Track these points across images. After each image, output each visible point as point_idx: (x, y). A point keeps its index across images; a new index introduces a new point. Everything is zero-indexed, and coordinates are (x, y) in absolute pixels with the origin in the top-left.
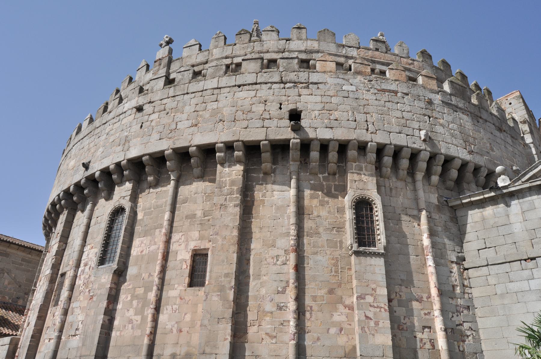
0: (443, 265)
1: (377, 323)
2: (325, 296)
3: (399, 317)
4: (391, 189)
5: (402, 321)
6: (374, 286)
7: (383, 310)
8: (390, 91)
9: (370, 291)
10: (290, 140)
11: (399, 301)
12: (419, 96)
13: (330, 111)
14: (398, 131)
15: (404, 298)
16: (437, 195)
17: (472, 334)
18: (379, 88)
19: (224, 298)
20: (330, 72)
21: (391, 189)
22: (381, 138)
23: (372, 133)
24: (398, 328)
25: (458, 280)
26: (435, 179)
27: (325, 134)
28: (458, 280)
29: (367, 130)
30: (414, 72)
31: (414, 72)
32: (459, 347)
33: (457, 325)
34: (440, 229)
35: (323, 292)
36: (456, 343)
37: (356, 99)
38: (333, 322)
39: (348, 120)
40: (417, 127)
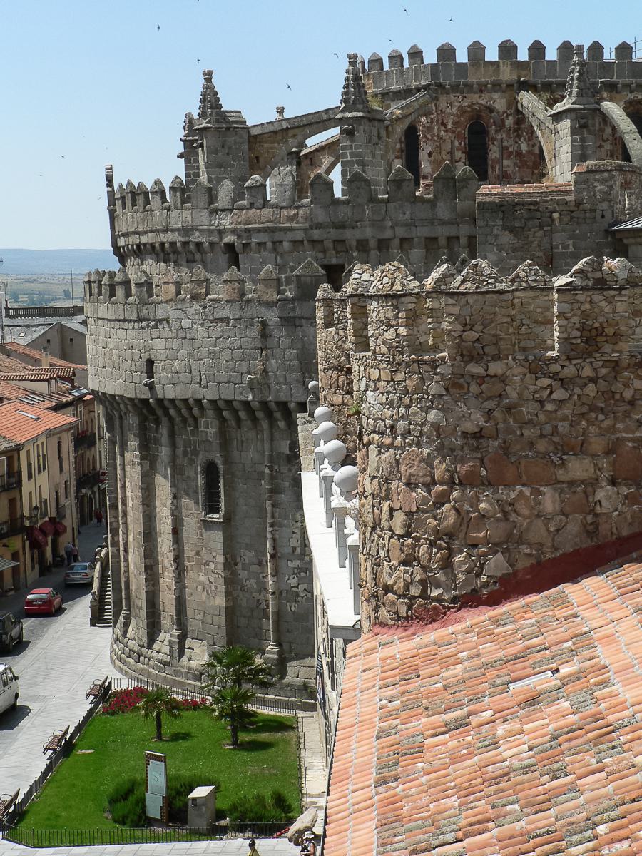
0: (284, 526)
1: (216, 587)
2: (195, 557)
3: (242, 579)
4: (242, 442)
5: (244, 583)
6: (214, 554)
7: (220, 576)
8: (221, 320)
9: (212, 559)
10: (149, 400)
11: (243, 564)
12: (253, 319)
13: (172, 360)
14: (226, 380)
15: (247, 561)
16: (289, 442)
17: (306, 595)
18: (211, 318)
19: (140, 555)
20: (172, 300)
21: (242, 442)
22: (209, 394)
23: (204, 387)
24: (241, 590)
25: (299, 542)
26: (282, 424)
27: (169, 393)
28: (299, 542)
29: (200, 383)
30: (298, 230)
31: (298, 230)
32: (290, 608)
33: (292, 587)
34: (287, 484)
35: (192, 554)
36: (288, 604)
37: (192, 339)
38: (199, 581)
39: (185, 372)
40: (245, 370)
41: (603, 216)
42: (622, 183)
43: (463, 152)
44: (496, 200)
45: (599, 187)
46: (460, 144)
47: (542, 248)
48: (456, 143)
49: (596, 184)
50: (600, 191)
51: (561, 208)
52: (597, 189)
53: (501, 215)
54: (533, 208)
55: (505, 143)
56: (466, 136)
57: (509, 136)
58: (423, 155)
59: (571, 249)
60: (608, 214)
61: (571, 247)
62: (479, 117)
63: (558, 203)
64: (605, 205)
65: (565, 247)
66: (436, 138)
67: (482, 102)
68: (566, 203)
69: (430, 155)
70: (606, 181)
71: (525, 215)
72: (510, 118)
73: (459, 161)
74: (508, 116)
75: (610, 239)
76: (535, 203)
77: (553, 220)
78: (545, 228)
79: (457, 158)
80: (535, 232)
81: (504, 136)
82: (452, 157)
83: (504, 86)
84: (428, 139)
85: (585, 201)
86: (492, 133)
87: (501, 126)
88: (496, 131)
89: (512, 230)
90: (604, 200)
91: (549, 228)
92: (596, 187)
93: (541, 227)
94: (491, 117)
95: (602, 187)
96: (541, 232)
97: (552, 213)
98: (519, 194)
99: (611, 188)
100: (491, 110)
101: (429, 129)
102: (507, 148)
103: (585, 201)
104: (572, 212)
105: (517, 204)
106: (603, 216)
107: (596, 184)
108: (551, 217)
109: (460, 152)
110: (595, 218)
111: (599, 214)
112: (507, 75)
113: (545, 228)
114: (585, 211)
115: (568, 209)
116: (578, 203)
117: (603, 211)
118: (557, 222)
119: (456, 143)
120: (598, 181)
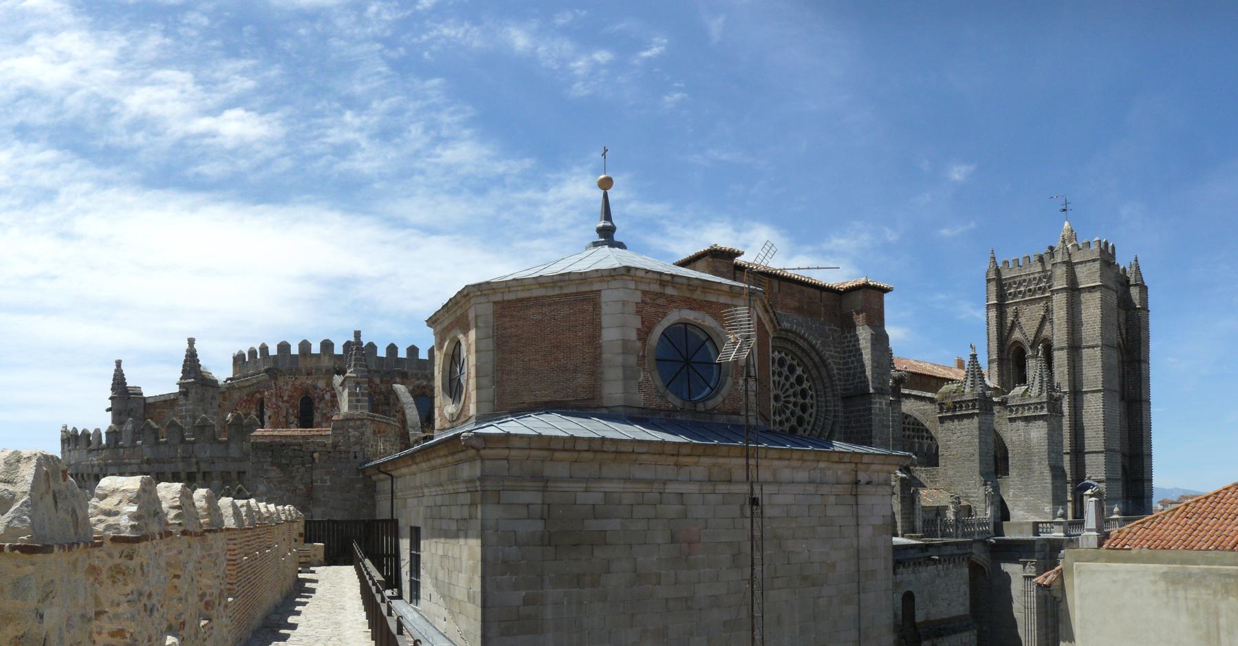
41: (356, 457)
42: (374, 431)
43: (295, 417)
44: (267, 441)
45: (352, 432)
46: (293, 411)
47: (304, 481)
48: (291, 411)
49: (350, 430)
50: (353, 436)
51: (321, 449)
52: (351, 434)
53: (270, 453)
54: (296, 448)
55: (325, 411)
56: (299, 405)
57: (327, 405)
58: (266, 418)
59: (328, 483)
60: (360, 455)
61: (328, 481)
62: (307, 392)
63: (318, 444)
64: (357, 448)
65: (323, 481)
66: (274, 406)
67: (308, 382)
68: (325, 445)
69: (270, 417)
70: (359, 428)
71: (291, 454)
72: (328, 393)
73: (292, 423)
74: (327, 391)
75: (361, 476)
76: (300, 445)
77: (313, 459)
78: (307, 466)
79: (291, 421)
80: (298, 469)
81: (324, 406)
82: (287, 420)
83: (324, 370)
84: (269, 407)
85: (340, 444)
86: (316, 405)
87: (322, 399)
88: (319, 402)
89: (280, 466)
90: (356, 443)
91: (310, 465)
92: (350, 432)
93: (303, 465)
94: (316, 393)
95: (355, 433)
96: (303, 469)
97: (313, 453)
98: (286, 436)
99: (363, 434)
100: (315, 388)
101: (270, 399)
102: (325, 414)
103: (340, 444)
104: (330, 452)
105: (284, 445)
106: (356, 457)
107: (350, 430)
108: (312, 456)
109: (293, 417)
110: (348, 458)
111: (351, 455)
112: (326, 363)
113: (307, 466)
114: (340, 452)
115: (326, 450)
116: (335, 446)
117: (355, 453)
118: (317, 461)
119: (291, 411)
120: (352, 428)
